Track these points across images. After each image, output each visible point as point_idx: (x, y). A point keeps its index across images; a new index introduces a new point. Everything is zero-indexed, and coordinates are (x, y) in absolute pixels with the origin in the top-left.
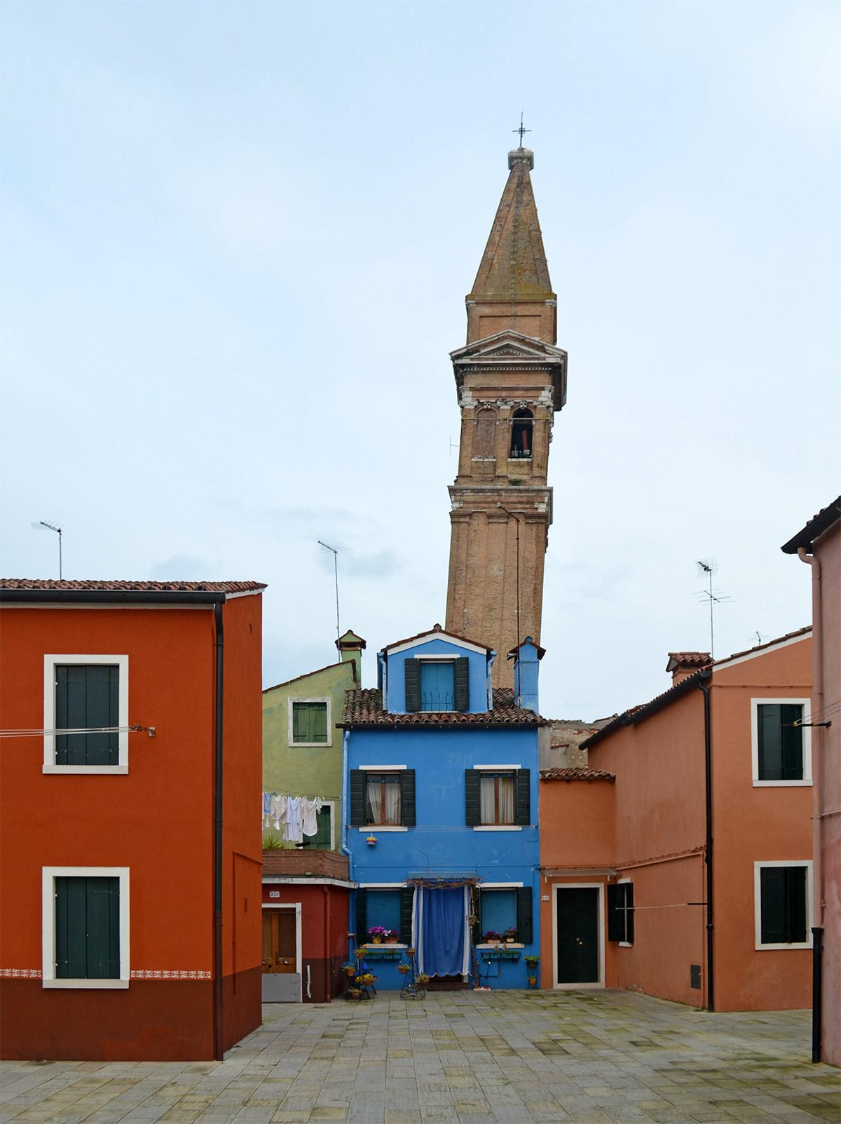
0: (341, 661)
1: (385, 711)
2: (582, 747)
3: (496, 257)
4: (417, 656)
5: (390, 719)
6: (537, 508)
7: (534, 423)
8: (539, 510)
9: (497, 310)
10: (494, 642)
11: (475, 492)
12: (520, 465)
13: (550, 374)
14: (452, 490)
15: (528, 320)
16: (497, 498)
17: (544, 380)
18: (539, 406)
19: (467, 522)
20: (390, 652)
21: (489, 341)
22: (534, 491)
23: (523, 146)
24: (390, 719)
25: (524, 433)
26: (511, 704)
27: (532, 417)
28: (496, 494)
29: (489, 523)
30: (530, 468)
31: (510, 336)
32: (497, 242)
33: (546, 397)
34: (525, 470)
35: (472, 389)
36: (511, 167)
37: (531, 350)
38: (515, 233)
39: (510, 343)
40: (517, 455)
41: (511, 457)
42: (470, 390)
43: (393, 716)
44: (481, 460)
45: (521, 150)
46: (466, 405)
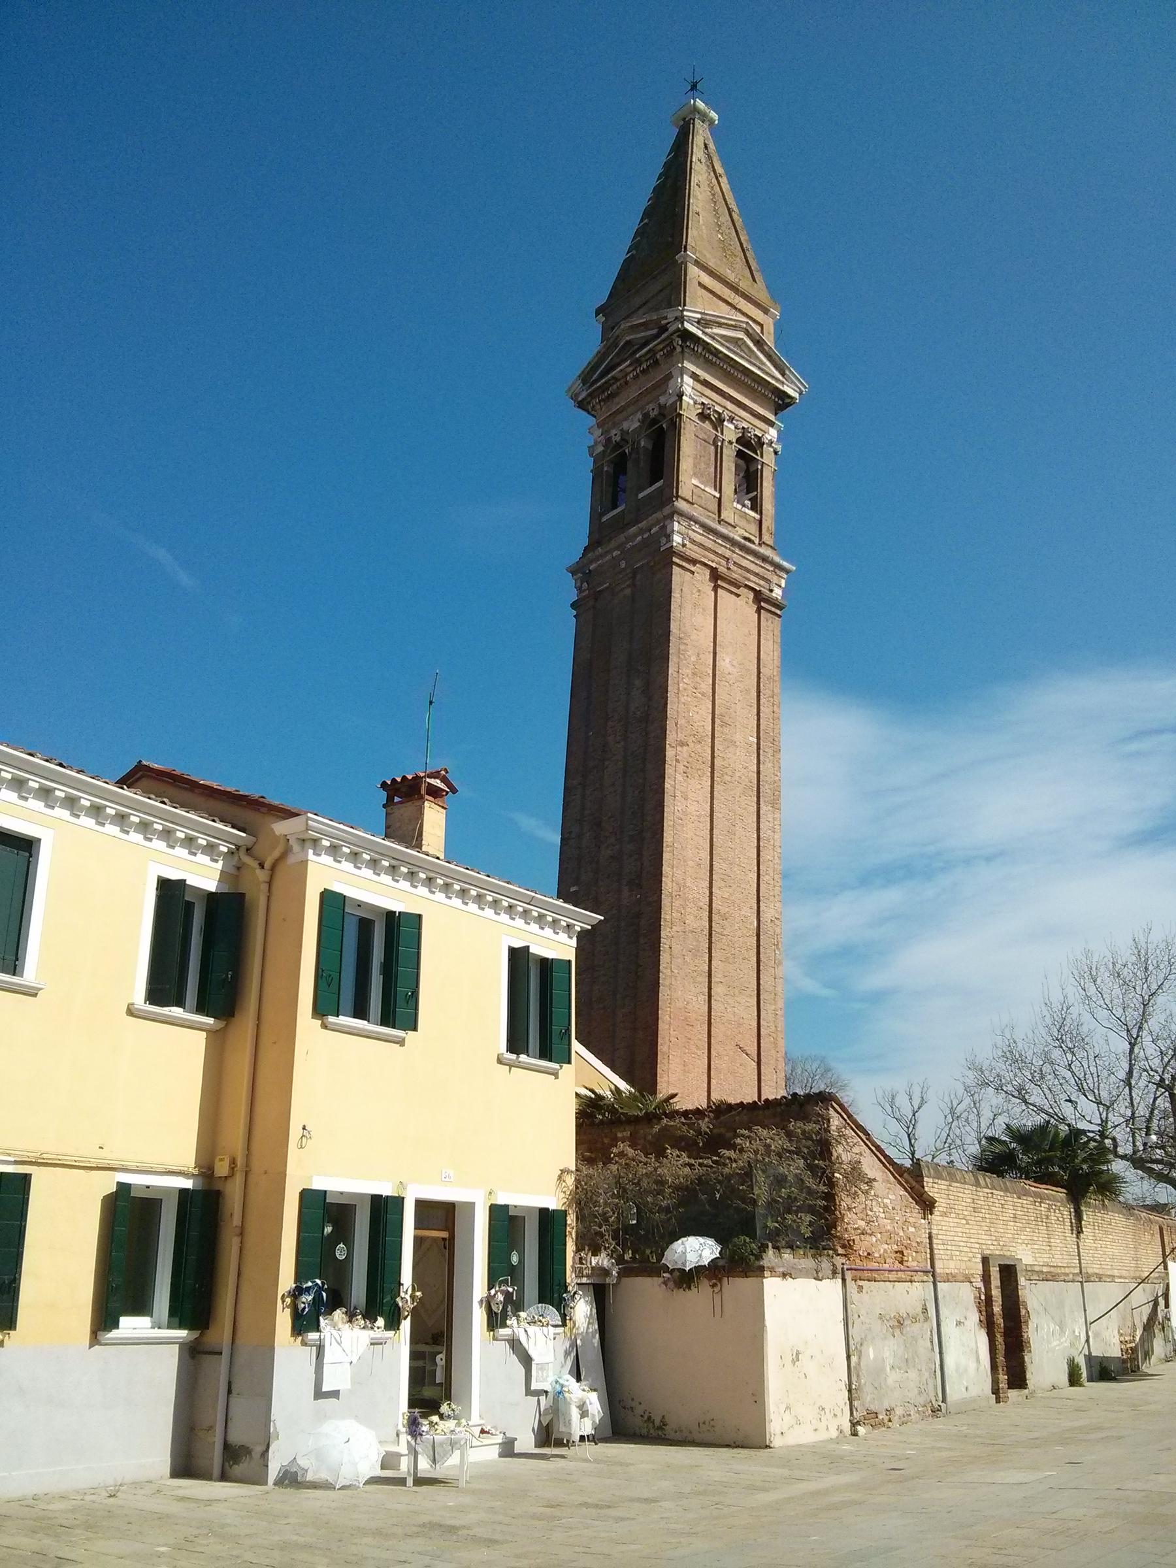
16: (728, 554)
21: (726, 321)
42: (691, 377)
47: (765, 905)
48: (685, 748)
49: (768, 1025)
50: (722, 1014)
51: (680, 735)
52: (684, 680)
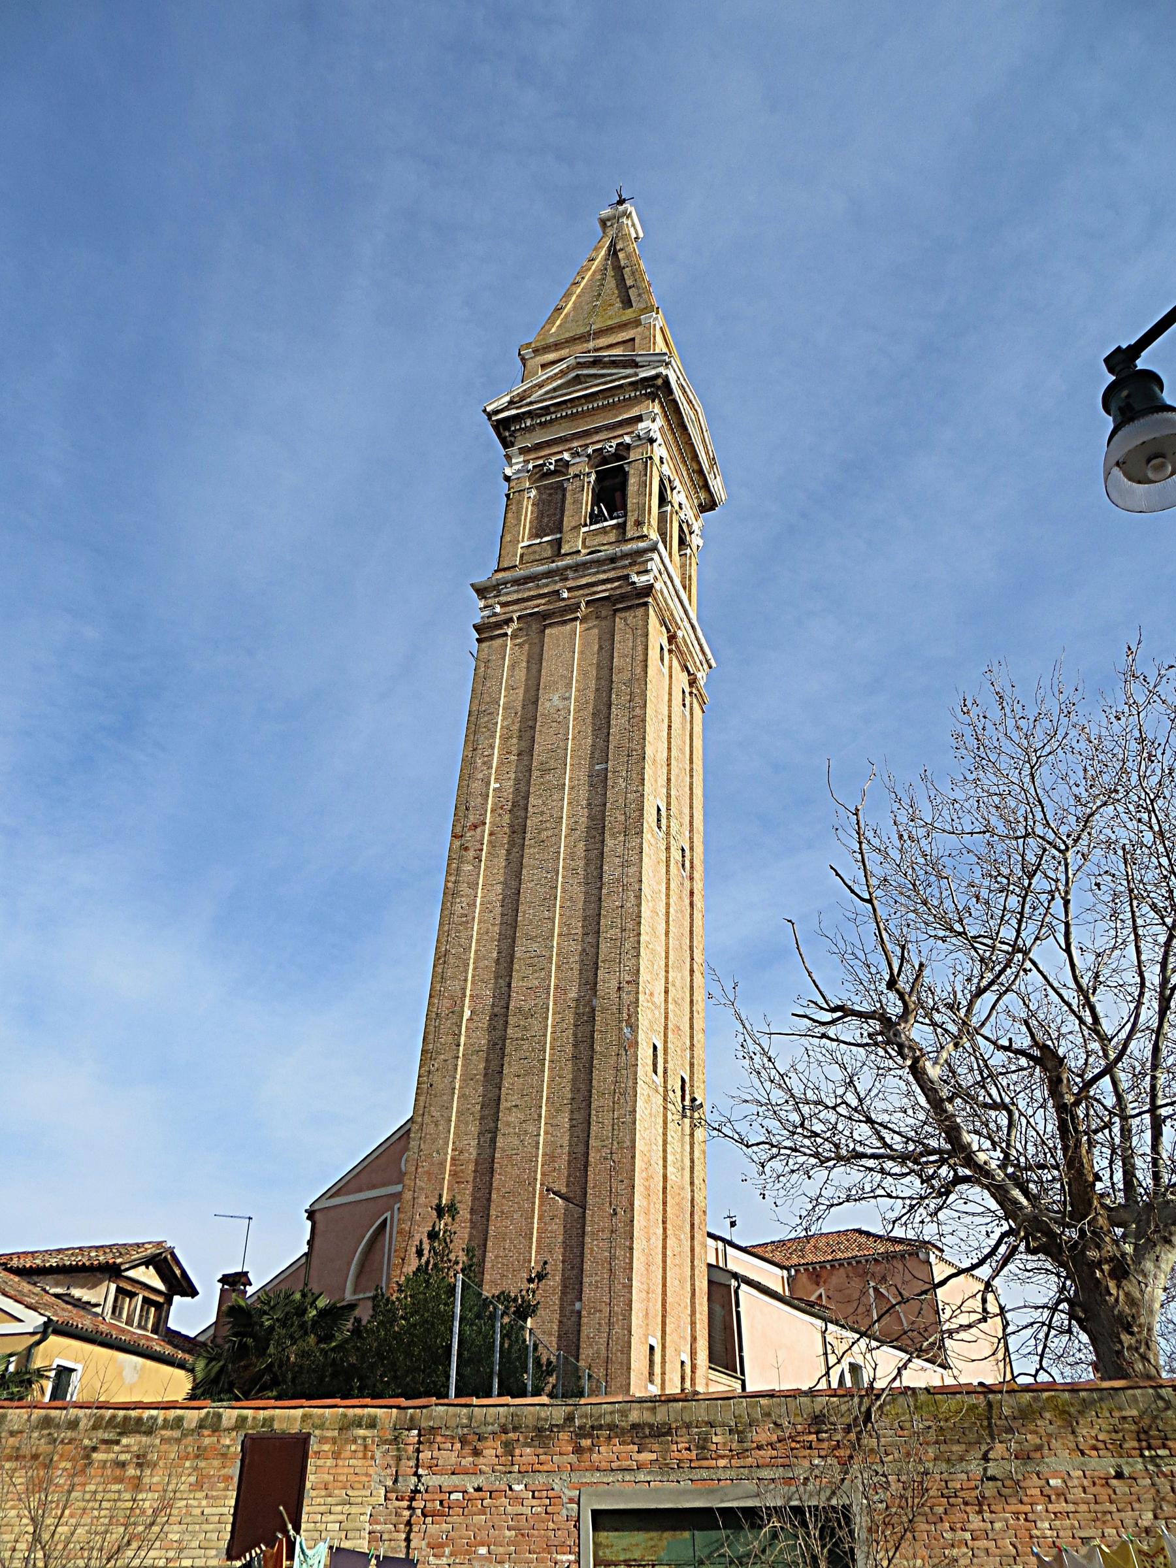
10: (550, 833)
12: (604, 531)
47: (607, 970)
49: (604, 1143)
50: (514, 1152)
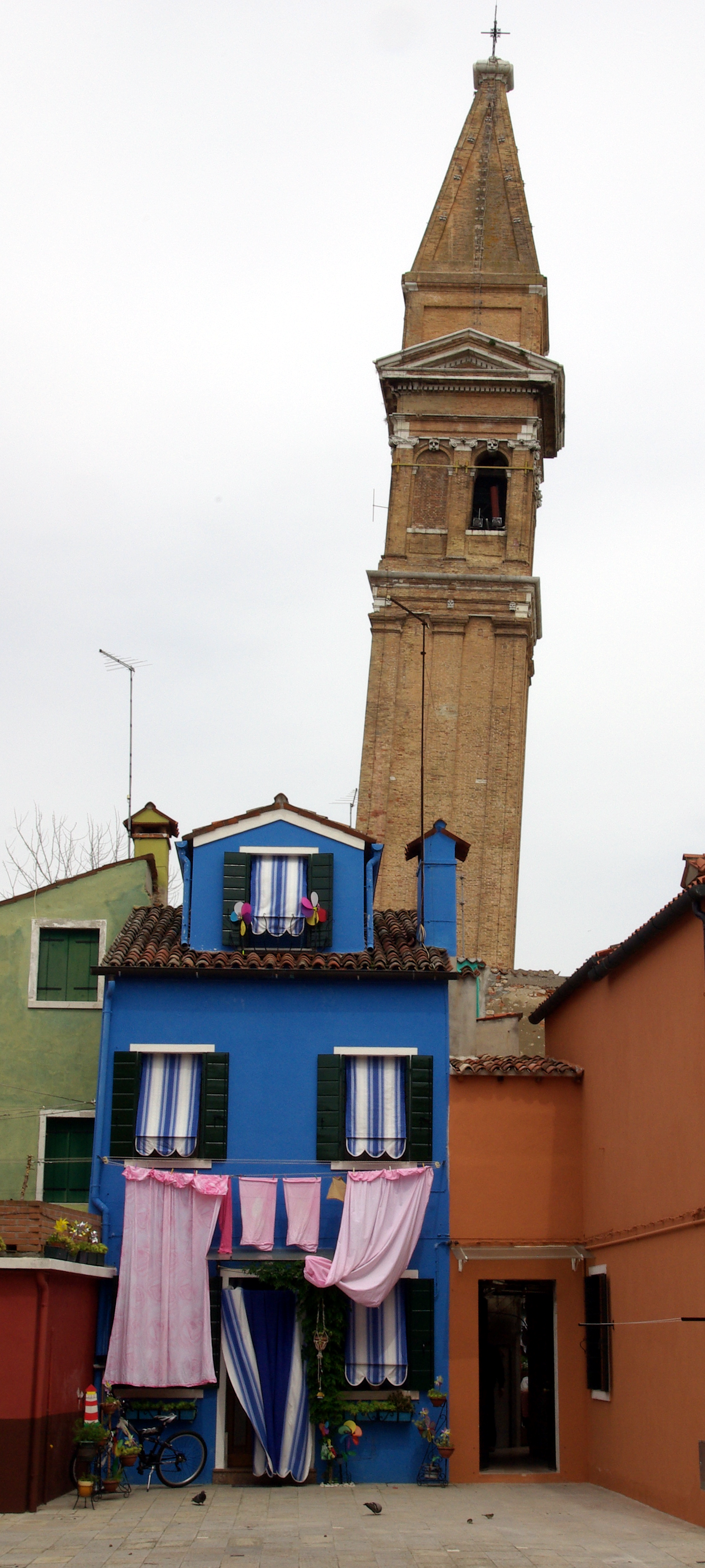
0: (132, 856)
1: (185, 945)
2: (534, 1018)
3: (452, 217)
4: (244, 850)
5: (189, 961)
6: (513, 612)
7: (509, 475)
8: (518, 615)
9: (451, 299)
11: (411, 583)
12: (485, 540)
13: (535, 399)
14: (374, 579)
15: (501, 315)
17: (527, 408)
18: (517, 449)
19: (398, 632)
20: (197, 842)
21: (437, 344)
22: (507, 583)
23: (497, 55)
24: (189, 961)
25: (494, 490)
26: (412, 938)
27: (507, 466)
28: (446, 586)
29: (434, 633)
30: (502, 546)
31: (471, 338)
32: (453, 195)
33: (528, 434)
34: (494, 549)
35: (409, 418)
36: (477, 85)
37: (505, 361)
38: (482, 184)
39: (471, 349)
40: (481, 524)
41: (473, 527)
42: (407, 421)
43: (197, 956)
44: (423, 531)
45: (494, 60)
46: (400, 443)
48: (381, 817)
51: (374, 805)
52: (383, 747)
